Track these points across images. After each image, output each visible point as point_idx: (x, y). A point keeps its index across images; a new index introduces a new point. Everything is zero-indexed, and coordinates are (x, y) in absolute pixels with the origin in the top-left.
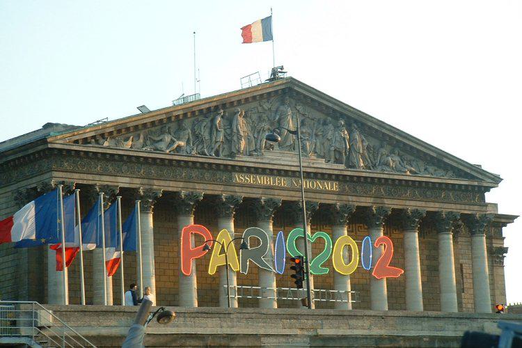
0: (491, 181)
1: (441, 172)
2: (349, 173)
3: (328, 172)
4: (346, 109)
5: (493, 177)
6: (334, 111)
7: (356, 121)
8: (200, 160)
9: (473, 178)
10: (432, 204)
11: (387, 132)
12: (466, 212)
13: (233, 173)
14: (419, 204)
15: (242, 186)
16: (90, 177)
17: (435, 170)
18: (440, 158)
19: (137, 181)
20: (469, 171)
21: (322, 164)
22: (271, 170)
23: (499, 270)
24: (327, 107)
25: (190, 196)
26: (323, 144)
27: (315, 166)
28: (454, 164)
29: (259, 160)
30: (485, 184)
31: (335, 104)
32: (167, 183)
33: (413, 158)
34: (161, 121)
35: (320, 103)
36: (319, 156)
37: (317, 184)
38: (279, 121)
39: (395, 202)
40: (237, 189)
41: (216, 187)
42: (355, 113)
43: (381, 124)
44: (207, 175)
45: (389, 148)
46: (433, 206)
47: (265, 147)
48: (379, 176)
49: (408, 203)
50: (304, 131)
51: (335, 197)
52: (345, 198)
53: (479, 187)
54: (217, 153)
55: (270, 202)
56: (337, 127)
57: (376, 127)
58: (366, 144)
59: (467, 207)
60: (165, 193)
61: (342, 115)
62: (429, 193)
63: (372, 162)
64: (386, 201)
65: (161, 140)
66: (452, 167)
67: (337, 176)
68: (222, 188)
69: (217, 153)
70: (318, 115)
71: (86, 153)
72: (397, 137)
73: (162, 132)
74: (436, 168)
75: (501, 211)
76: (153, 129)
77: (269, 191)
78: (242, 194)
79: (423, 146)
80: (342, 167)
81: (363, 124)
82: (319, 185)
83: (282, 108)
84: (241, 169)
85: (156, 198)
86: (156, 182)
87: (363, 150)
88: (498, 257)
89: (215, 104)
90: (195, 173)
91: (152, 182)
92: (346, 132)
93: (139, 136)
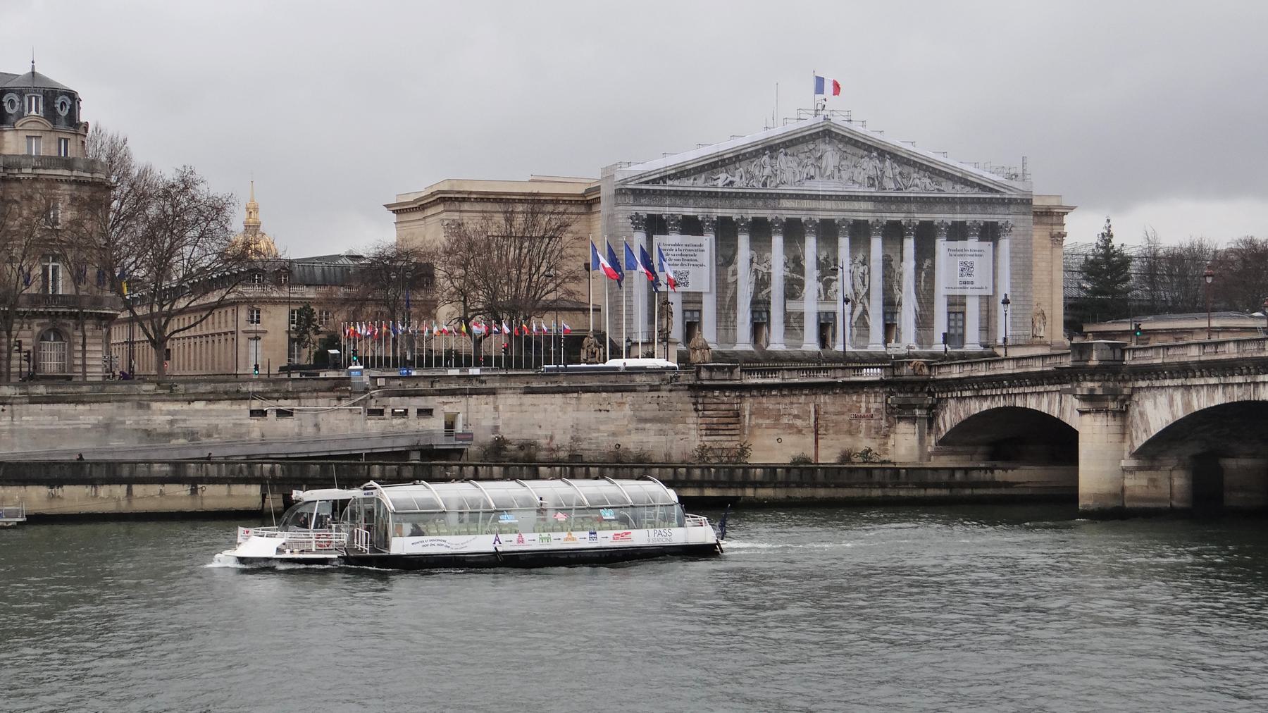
1: (968, 189)
7: (889, 153)
15: (788, 209)
25: (742, 219)
38: (820, 158)
44: (760, 203)
45: (922, 173)
46: (959, 217)
54: (765, 185)
55: (810, 221)
58: (898, 170)
61: (876, 149)
66: (979, 185)
69: (765, 185)
71: (655, 191)
78: (785, 215)
80: (873, 189)
81: (896, 155)
83: (822, 146)
84: (784, 196)
87: (895, 176)
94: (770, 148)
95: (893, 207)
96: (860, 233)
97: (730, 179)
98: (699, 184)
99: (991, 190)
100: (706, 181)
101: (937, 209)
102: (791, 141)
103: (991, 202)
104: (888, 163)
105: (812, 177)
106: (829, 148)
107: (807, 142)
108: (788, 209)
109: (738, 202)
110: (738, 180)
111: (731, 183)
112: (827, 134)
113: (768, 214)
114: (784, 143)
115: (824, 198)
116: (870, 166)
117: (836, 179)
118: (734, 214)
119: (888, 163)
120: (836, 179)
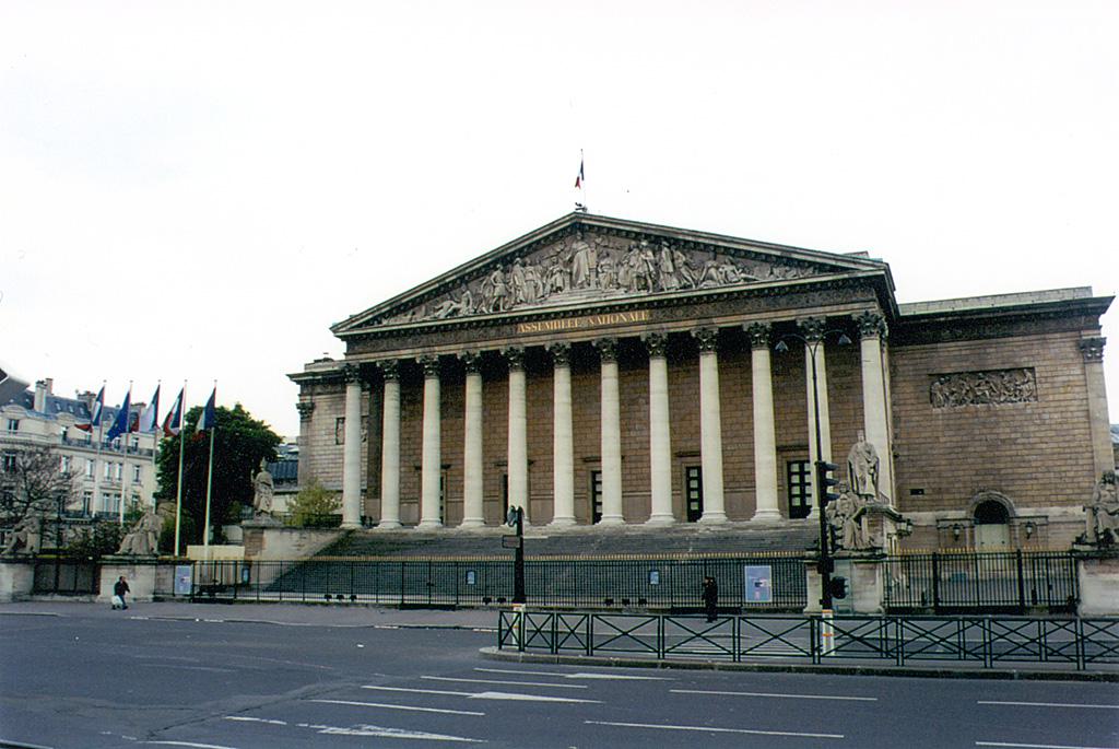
1: (794, 272)
2: (653, 298)
3: (627, 302)
6: (638, 234)
7: (666, 239)
8: (472, 319)
10: (786, 313)
11: (707, 241)
12: (841, 314)
14: (764, 315)
15: (528, 335)
16: (376, 355)
19: (420, 350)
20: (833, 263)
21: (620, 295)
22: (557, 314)
23: (1096, 367)
24: (628, 232)
26: (627, 272)
28: (810, 259)
29: (539, 306)
30: (860, 275)
32: (448, 347)
33: (758, 263)
35: (619, 230)
36: (619, 286)
37: (620, 318)
39: (729, 319)
40: (522, 340)
41: (500, 342)
43: (694, 233)
44: (493, 332)
45: (720, 257)
46: (784, 316)
48: (695, 294)
49: (747, 317)
50: (602, 263)
51: (644, 327)
52: (657, 326)
54: (496, 308)
56: (641, 250)
57: (690, 238)
59: (842, 307)
60: (440, 357)
61: (647, 237)
62: (783, 300)
64: (715, 320)
65: (442, 308)
66: (811, 264)
67: (641, 304)
68: (506, 341)
69: (496, 308)
70: (624, 242)
71: (368, 334)
72: (720, 244)
73: (443, 300)
74: (787, 268)
75: (1096, 294)
77: (559, 336)
80: (644, 293)
81: (677, 241)
82: (623, 317)
83: (574, 246)
84: (521, 319)
85: (435, 363)
86: (436, 348)
88: (1091, 352)
89: (489, 260)
90: (474, 333)
91: (432, 349)
92: (650, 253)
93: (420, 309)
94: (504, 259)
95: (680, 313)
96: (632, 357)
97: (455, 306)
98: (420, 319)
99: (834, 269)
101: (749, 307)
102: (530, 246)
103: (836, 285)
105: (560, 289)
106: (580, 246)
107: (553, 242)
110: (464, 307)
111: (456, 311)
112: (578, 227)
113: (502, 346)
114: (521, 250)
115: (575, 313)
116: (641, 260)
117: (593, 286)
118: (457, 350)
120: (593, 286)
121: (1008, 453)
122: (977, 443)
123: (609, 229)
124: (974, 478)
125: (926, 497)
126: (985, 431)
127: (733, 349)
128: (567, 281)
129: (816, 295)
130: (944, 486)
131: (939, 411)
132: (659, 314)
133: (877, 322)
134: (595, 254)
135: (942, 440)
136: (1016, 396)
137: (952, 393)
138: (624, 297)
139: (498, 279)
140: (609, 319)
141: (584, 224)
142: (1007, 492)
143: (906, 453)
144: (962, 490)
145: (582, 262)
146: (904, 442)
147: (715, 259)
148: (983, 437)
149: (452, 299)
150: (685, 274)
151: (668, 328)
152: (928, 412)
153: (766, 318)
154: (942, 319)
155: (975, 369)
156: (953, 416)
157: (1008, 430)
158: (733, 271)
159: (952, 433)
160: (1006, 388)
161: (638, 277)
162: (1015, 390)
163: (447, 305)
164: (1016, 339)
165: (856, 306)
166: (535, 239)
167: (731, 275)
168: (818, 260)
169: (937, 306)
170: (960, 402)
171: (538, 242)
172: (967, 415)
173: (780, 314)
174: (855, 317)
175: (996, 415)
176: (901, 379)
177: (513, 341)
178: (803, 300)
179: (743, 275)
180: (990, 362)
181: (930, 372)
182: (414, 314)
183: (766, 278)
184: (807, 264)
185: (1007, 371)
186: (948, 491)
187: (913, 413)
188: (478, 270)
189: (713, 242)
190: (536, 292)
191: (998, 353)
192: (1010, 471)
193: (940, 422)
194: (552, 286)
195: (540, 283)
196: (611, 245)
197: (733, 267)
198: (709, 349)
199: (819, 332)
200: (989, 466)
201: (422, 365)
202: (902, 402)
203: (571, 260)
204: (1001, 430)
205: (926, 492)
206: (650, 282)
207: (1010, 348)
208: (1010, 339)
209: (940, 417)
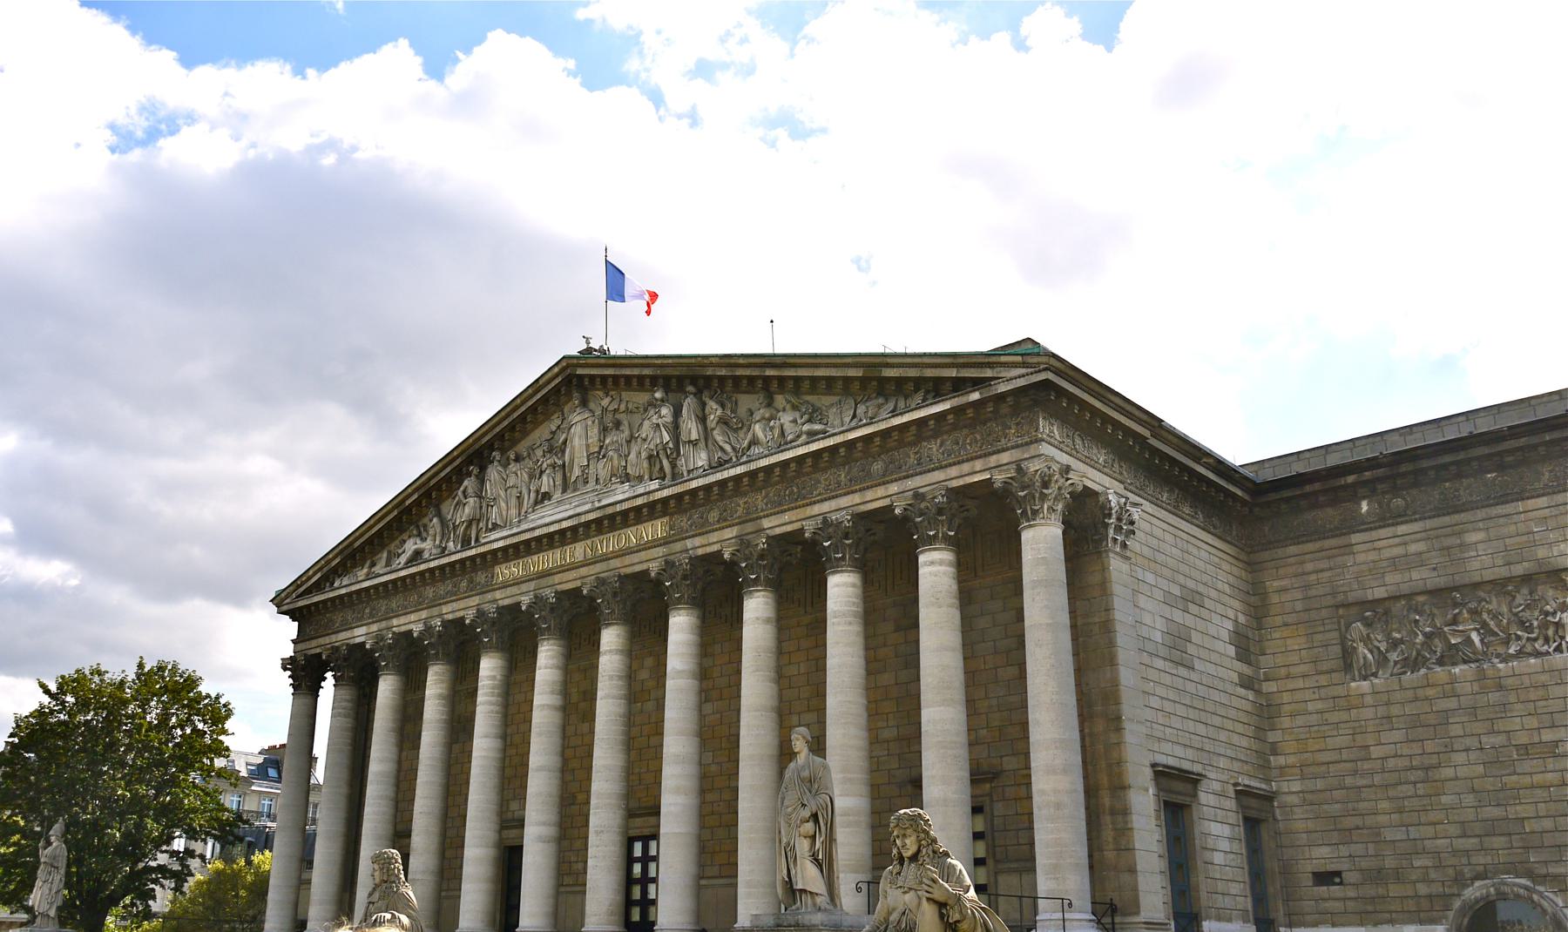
0: (1023, 371)
1: (891, 406)
2: (666, 493)
4: (662, 366)
5: (1019, 359)
7: (694, 380)
9: (977, 383)
10: (880, 492)
11: (748, 372)
12: (976, 478)
13: (497, 569)
14: (844, 501)
17: (879, 406)
18: (873, 373)
19: (374, 628)
20: (953, 373)
21: (621, 495)
25: (428, 629)
27: (604, 502)
28: (912, 373)
29: (515, 530)
31: (643, 366)
34: (398, 519)
35: (628, 378)
39: (786, 517)
40: (498, 595)
42: (681, 365)
43: (728, 360)
45: (780, 400)
47: (536, 503)
52: (678, 546)
53: (1002, 397)
55: (538, 601)
59: (978, 465)
63: (734, 448)
64: (766, 523)
66: (919, 382)
67: (651, 506)
70: (642, 398)
72: (770, 372)
74: (881, 400)
76: (405, 536)
77: (544, 582)
79: (827, 366)
80: (654, 485)
82: (631, 536)
89: (458, 461)
90: (442, 589)
95: (713, 516)
98: (382, 573)
100: (388, 564)
102: (511, 427)
104: (689, 404)
105: (547, 496)
108: (504, 586)
109: (429, 592)
111: (417, 556)
112: (580, 381)
118: (412, 623)
119: (689, 404)
120: (591, 485)
121: (1537, 778)
122: (1460, 758)
123: (616, 378)
124: (1461, 843)
125: (1352, 893)
126: (1479, 728)
127: (797, 572)
128: (559, 482)
129: (934, 446)
130: (1390, 863)
131: (1365, 685)
132: (683, 521)
133: (1046, 485)
134: (596, 430)
135: (1376, 752)
136: (1547, 641)
137: (1395, 644)
138: (627, 495)
139: (470, 490)
140: (609, 543)
141: (581, 377)
142: (1543, 879)
143: (1296, 786)
144: (1433, 875)
145: (576, 442)
146: (1291, 760)
147: (769, 405)
148: (1472, 742)
149: (419, 535)
150: (719, 438)
151: (695, 548)
152: (1339, 691)
153: (841, 507)
154: (1351, 479)
155: (1441, 582)
156: (1398, 696)
157: (1533, 722)
158: (795, 421)
159: (1398, 735)
160: (1522, 624)
161: (650, 457)
162: (1544, 625)
163: (411, 546)
164: (1531, 503)
165: (1005, 457)
166: (515, 415)
167: (788, 427)
168: (929, 373)
169: (1348, 453)
170: (1412, 663)
171: (523, 417)
172: (1430, 692)
173: (869, 495)
174: (999, 478)
175: (1500, 688)
176: (1279, 620)
177: (489, 596)
178: (912, 460)
179: (806, 428)
180: (1476, 565)
181: (1341, 597)
182: (373, 565)
183: (847, 425)
184: (911, 386)
185: (1527, 579)
186: (1398, 876)
187: (1308, 695)
188: (447, 479)
189: (756, 372)
190: (520, 505)
191: (1486, 543)
192: (1548, 824)
193: (1368, 713)
194: (537, 492)
195: (525, 491)
196: (623, 407)
197: (797, 415)
198: (756, 582)
199: (933, 523)
200: (1496, 812)
201: (373, 651)
202: (1283, 671)
203: (565, 442)
204: (1516, 724)
205: (1350, 877)
206: (665, 462)
207: (1522, 528)
208: (1521, 506)
209: (1369, 700)
